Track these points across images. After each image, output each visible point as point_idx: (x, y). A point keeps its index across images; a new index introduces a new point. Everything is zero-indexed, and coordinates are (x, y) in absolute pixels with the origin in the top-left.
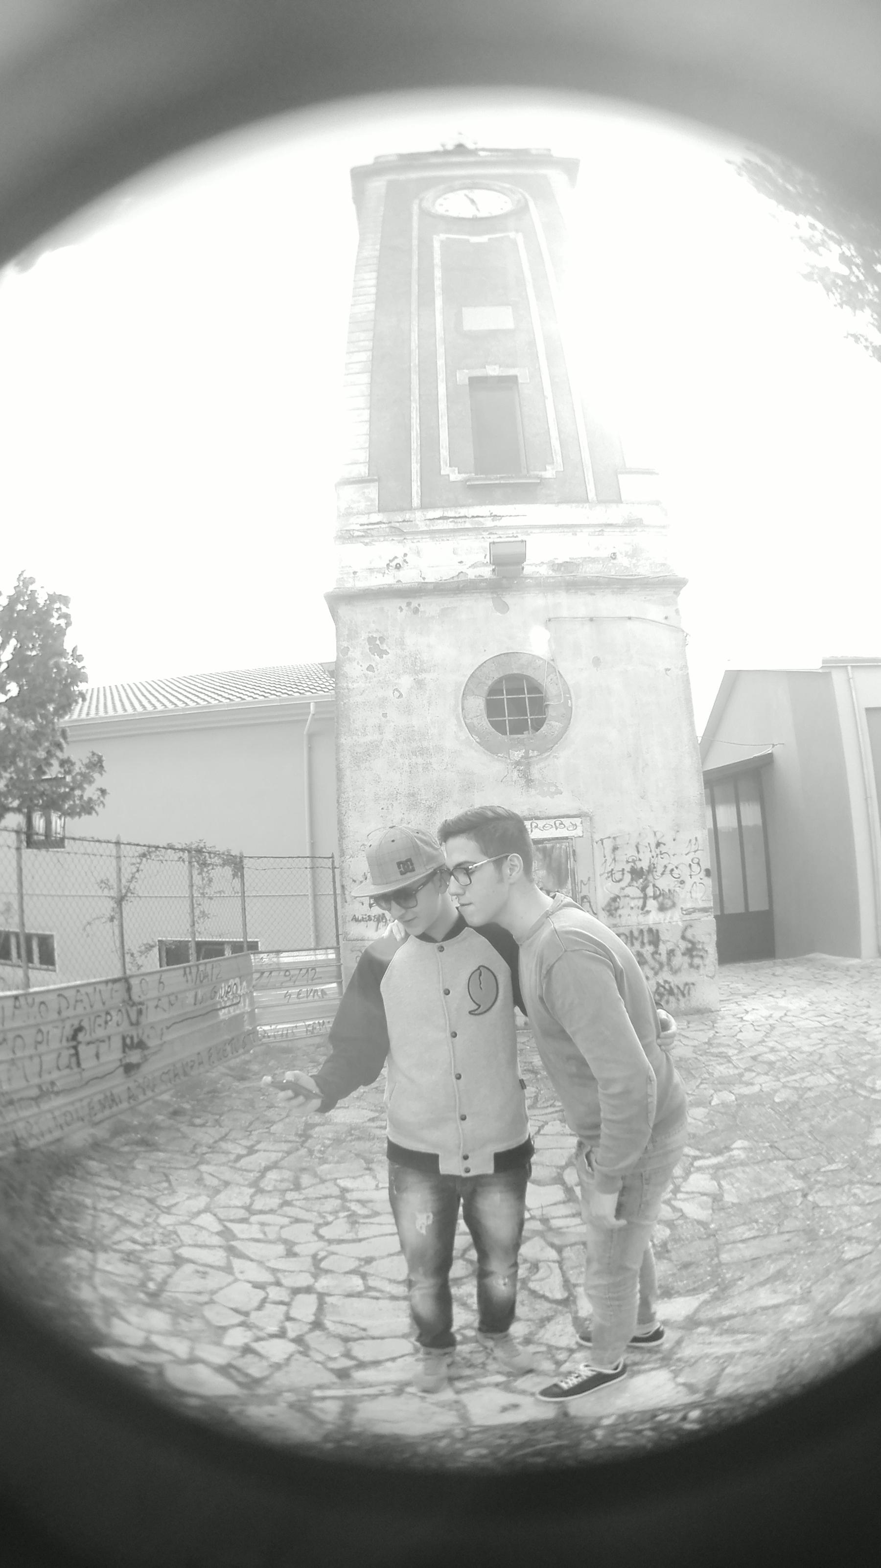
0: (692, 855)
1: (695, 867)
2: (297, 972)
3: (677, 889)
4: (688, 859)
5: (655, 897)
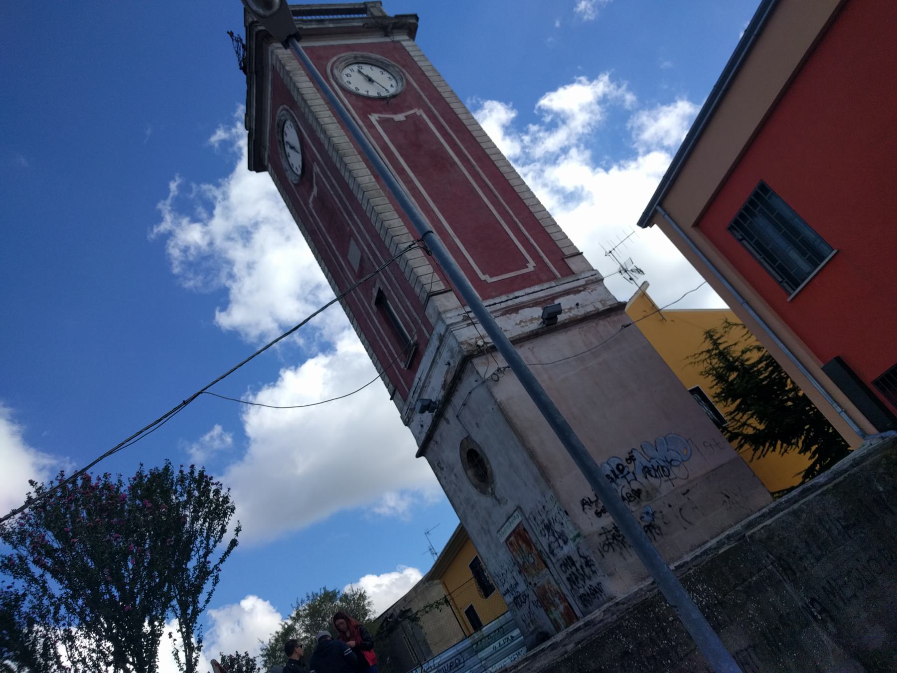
0: (556, 508)
1: (560, 512)
2: (494, 634)
3: (563, 529)
4: (556, 510)
5: (560, 537)
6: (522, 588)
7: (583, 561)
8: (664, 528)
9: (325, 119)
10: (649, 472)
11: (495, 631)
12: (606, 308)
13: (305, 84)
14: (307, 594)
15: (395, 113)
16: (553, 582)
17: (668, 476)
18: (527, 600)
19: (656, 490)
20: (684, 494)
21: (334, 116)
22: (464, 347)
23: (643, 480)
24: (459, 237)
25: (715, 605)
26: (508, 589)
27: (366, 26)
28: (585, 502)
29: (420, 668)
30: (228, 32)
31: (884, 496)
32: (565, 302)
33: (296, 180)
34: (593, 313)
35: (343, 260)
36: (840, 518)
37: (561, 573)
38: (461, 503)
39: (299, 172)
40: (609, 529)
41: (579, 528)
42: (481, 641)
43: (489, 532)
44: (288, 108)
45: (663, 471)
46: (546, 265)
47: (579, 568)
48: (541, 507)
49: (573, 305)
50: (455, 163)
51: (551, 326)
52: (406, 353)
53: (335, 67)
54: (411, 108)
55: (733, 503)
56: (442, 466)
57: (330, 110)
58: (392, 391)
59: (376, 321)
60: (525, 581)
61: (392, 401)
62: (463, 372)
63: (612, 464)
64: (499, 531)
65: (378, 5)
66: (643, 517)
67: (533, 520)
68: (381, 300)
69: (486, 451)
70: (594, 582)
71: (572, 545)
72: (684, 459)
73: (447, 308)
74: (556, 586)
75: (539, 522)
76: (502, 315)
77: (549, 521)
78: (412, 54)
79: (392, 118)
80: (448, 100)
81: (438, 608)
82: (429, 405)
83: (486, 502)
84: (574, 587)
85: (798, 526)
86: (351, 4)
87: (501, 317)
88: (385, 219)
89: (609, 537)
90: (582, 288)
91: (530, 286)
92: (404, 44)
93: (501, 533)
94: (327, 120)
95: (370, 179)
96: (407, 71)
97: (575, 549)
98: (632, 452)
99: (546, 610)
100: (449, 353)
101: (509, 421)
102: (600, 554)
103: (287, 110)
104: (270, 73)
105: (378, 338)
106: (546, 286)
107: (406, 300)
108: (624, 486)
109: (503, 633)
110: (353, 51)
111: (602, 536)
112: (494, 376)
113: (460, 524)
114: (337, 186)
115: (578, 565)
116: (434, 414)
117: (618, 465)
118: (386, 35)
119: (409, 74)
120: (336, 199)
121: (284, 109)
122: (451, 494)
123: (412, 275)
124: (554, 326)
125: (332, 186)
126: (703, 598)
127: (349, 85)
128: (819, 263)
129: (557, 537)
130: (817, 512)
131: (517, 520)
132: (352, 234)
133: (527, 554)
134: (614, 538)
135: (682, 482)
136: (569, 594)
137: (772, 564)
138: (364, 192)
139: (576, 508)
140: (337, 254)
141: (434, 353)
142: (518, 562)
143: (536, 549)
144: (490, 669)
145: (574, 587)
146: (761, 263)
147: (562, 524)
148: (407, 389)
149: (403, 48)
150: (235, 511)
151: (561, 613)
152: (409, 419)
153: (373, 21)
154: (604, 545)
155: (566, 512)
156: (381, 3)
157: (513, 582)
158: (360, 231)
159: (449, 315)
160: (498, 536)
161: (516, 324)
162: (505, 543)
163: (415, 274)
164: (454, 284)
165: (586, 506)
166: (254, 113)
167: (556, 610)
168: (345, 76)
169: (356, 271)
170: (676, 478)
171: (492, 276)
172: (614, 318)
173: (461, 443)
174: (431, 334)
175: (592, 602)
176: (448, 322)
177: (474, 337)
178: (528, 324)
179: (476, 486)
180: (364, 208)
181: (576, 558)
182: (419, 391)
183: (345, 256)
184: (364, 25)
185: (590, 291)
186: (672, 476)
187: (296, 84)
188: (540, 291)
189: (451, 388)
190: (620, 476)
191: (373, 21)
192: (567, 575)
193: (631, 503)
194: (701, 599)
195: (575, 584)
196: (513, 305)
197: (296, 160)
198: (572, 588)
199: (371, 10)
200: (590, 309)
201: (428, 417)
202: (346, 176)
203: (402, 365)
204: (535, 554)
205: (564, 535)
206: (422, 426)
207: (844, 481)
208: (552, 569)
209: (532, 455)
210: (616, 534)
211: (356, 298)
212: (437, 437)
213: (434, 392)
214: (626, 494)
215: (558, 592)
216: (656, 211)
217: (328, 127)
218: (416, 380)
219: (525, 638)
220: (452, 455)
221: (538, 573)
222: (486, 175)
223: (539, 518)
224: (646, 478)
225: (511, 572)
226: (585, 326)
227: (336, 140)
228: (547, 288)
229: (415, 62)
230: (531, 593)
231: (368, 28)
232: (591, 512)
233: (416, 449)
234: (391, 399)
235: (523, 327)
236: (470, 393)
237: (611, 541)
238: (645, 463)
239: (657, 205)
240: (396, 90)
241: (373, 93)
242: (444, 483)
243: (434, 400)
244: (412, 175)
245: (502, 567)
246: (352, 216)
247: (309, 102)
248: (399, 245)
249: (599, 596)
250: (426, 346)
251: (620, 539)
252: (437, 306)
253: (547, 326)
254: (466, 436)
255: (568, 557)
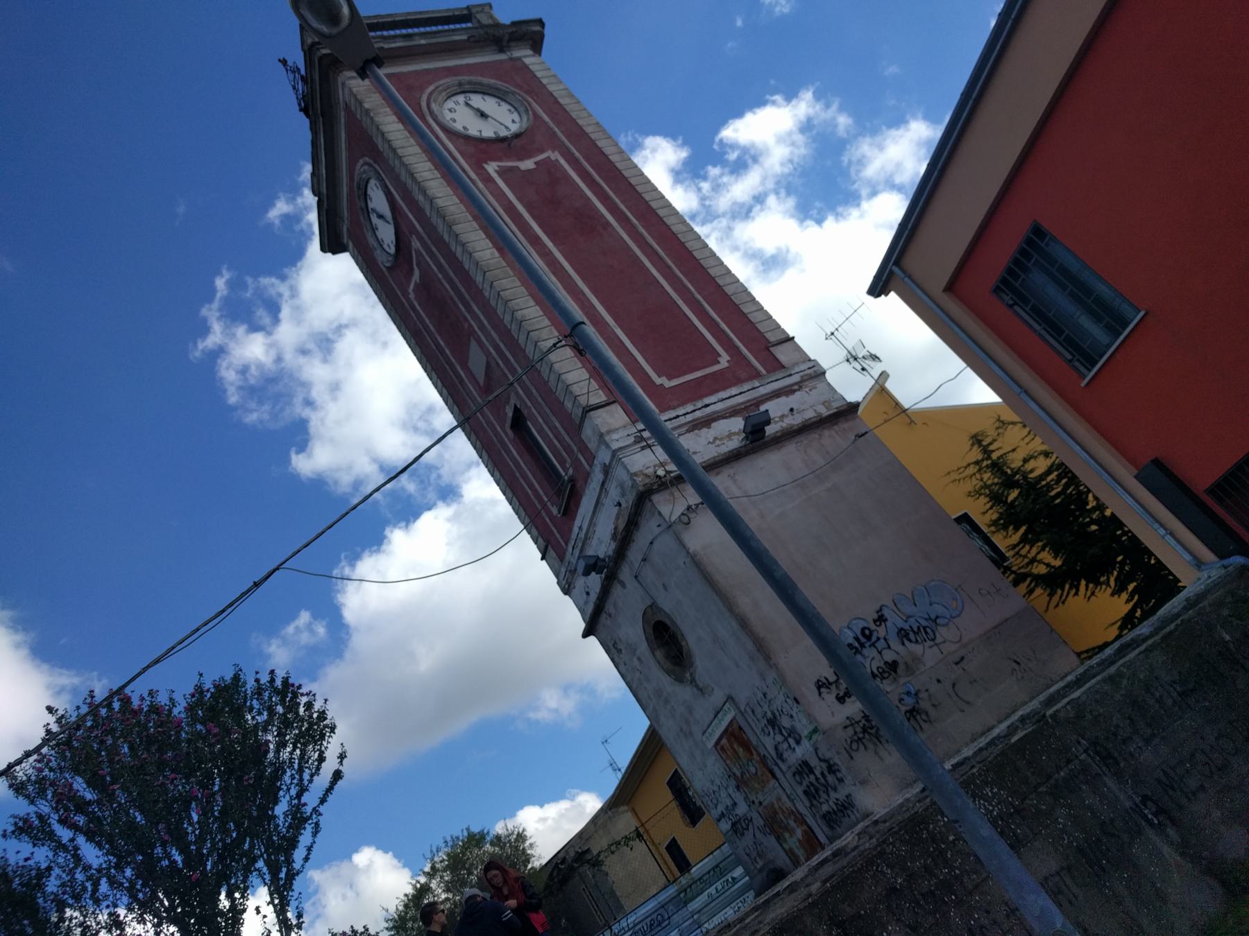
0: (781, 693)
1: (788, 700)
2: (708, 876)
3: (793, 723)
4: (781, 698)
5: (789, 736)
6: (742, 809)
7: (824, 765)
8: (932, 712)
9: (425, 174)
10: (907, 635)
11: (709, 872)
12: (831, 412)
13: (392, 127)
14: (444, 838)
15: (521, 159)
16: (785, 798)
17: (933, 640)
18: (751, 826)
19: (917, 659)
20: (957, 664)
21: (436, 169)
22: (639, 479)
23: (899, 648)
24: (621, 326)
25: (1011, 815)
26: (722, 813)
27: (472, 39)
28: (820, 683)
29: (609, 931)
30: (279, 60)
31: (1231, 646)
32: (775, 408)
33: (388, 261)
34: (813, 420)
35: (462, 369)
36: (1174, 682)
37: (794, 783)
38: (649, 697)
39: (392, 250)
40: (857, 719)
41: (816, 721)
42: (690, 886)
43: (691, 734)
44: (371, 161)
45: (926, 633)
46: (745, 358)
47: (819, 776)
48: (760, 695)
49: (786, 411)
50: (608, 224)
51: (757, 443)
52: (559, 493)
53: (432, 100)
54: (542, 151)
55: (1025, 670)
56: (619, 647)
57: (429, 160)
58: (543, 548)
59: (514, 452)
60: (746, 798)
61: (544, 561)
62: (640, 515)
63: (854, 629)
64: (704, 733)
65: (487, 9)
66: (903, 700)
67: (751, 713)
68: (519, 422)
69: (679, 622)
70: (841, 795)
71: (808, 746)
72: (954, 615)
73: (612, 427)
74: (789, 804)
75: (759, 716)
76: (688, 431)
77: (773, 714)
78: (539, 74)
79: (517, 167)
80: (593, 136)
81: (628, 845)
82: (596, 563)
83: (684, 693)
84: (815, 802)
85: (1118, 697)
86: (448, 10)
87: (687, 435)
88: (516, 308)
89: (859, 730)
90: (796, 387)
91: (724, 388)
92: (527, 61)
93: (707, 734)
94: (427, 175)
95: (492, 254)
96: (532, 98)
97: (812, 749)
98: (881, 610)
99: (778, 838)
100: (619, 490)
101: (708, 579)
102: (847, 755)
103: (369, 165)
104: (343, 113)
105: (518, 475)
106: (746, 387)
107: (554, 419)
108: (873, 659)
109: (721, 874)
110: (455, 75)
111: (848, 729)
112: (683, 517)
113: (650, 726)
114: (446, 266)
115: (818, 773)
116: (603, 576)
117: (863, 630)
118: (501, 50)
119: (537, 103)
120: (446, 285)
121: (366, 163)
122: (634, 686)
123: (560, 385)
124: (761, 441)
125: (440, 267)
126: (992, 805)
127: (454, 125)
128: (1121, 330)
129: (786, 735)
130: (1142, 677)
131: (728, 715)
132: (472, 332)
133: (746, 763)
134: (864, 730)
135: (953, 647)
136: (809, 815)
137: (1085, 751)
138: (485, 272)
139: (810, 693)
140: (453, 360)
141: (598, 491)
142: (734, 774)
143: (759, 754)
144: (706, 925)
145: (815, 802)
146: (1040, 336)
147: (792, 716)
148: (563, 544)
149: (526, 67)
150: (336, 731)
151: (799, 841)
152: (569, 586)
153: (481, 31)
154: (851, 742)
155: (796, 699)
156: (490, 6)
157: (729, 802)
158: (482, 327)
159: (615, 436)
160: (704, 738)
161: (709, 443)
162: (714, 749)
163: (563, 382)
164: (619, 393)
165: (823, 690)
166: (324, 172)
167: (791, 836)
168: (447, 111)
169: (482, 384)
170: (944, 642)
171: (670, 378)
172: (844, 425)
173: (644, 614)
174: (591, 465)
175: (841, 822)
176: (615, 446)
177: (652, 464)
178: (725, 442)
179: (669, 673)
180: (487, 294)
181: (814, 762)
182: (580, 545)
183: (464, 364)
184: (469, 38)
185: (807, 390)
186: (939, 640)
187: (380, 127)
188: (737, 395)
189: (624, 538)
190: (867, 645)
191: (481, 31)
192: (804, 787)
193: (884, 681)
194: (991, 808)
195: (815, 798)
196: (702, 417)
197: (386, 233)
198: (812, 805)
199: (478, 16)
200: (810, 414)
201: (595, 581)
202: (459, 252)
203: (554, 511)
204: (757, 762)
205: (796, 732)
206: (588, 593)
207: (1176, 629)
208: (782, 780)
209: (744, 623)
210: (867, 724)
211: (483, 422)
212: (609, 607)
213: (602, 545)
214: (878, 668)
215: (792, 812)
216: (891, 273)
217: (428, 184)
218: (576, 530)
219: (751, 878)
220: (633, 632)
221: (763, 787)
222: (653, 237)
223: (758, 710)
224: (903, 644)
225: (726, 789)
226: (804, 439)
227: (440, 203)
228: (748, 390)
229: (544, 86)
230: (755, 815)
231: (475, 42)
232: (830, 698)
233: (582, 626)
234: (542, 559)
235: (719, 446)
236: (651, 543)
237: (861, 736)
238: (901, 624)
239: (893, 265)
240: (521, 127)
241: (488, 133)
242: (624, 671)
243: (601, 556)
244: (550, 244)
245: (712, 782)
246: (471, 307)
247: (399, 151)
248: (539, 344)
249: (849, 812)
250: (586, 482)
251: (873, 731)
252: (597, 425)
253: (752, 442)
254: (649, 604)
255: (803, 762)
